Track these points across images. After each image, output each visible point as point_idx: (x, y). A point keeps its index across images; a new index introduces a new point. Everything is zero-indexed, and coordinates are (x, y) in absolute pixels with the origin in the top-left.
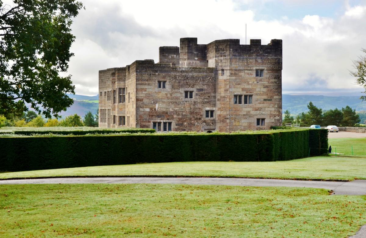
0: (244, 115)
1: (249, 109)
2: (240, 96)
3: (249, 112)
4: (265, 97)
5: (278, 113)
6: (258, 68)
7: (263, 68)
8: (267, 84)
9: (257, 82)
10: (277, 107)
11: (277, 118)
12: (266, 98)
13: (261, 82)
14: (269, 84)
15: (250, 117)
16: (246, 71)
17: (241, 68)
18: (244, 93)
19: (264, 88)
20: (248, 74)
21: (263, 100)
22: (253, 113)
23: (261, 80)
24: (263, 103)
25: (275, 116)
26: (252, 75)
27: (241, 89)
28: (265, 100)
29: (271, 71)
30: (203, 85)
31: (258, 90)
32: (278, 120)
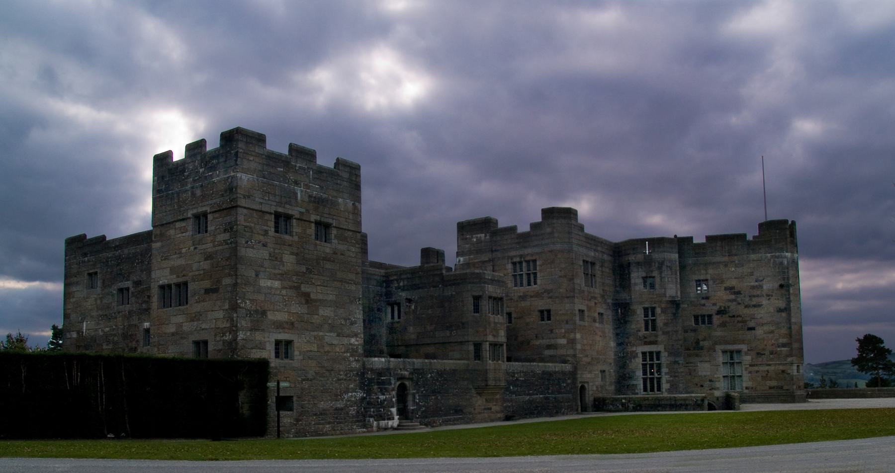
0: (173, 334)
1: (180, 319)
2: (169, 286)
3: (180, 325)
4: (207, 284)
5: (228, 325)
6: (195, 211)
7: (204, 209)
8: (210, 250)
9: (195, 248)
10: (227, 307)
11: (228, 337)
12: (208, 286)
13: (200, 247)
14: (214, 249)
15: (182, 338)
16: (178, 225)
17: (169, 219)
18: (173, 279)
19: (206, 259)
20: (180, 228)
21: (203, 291)
22: (186, 327)
23: (200, 242)
24: (204, 301)
25: (224, 334)
26: (186, 231)
27: (167, 271)
28: (207, 291)
29: (217, 215)
30: (142, 271)
31: (195, 266)
32: (230, 343)
